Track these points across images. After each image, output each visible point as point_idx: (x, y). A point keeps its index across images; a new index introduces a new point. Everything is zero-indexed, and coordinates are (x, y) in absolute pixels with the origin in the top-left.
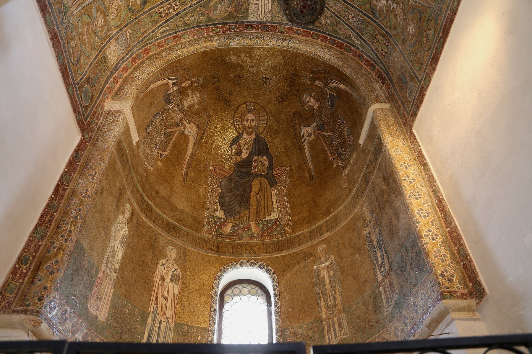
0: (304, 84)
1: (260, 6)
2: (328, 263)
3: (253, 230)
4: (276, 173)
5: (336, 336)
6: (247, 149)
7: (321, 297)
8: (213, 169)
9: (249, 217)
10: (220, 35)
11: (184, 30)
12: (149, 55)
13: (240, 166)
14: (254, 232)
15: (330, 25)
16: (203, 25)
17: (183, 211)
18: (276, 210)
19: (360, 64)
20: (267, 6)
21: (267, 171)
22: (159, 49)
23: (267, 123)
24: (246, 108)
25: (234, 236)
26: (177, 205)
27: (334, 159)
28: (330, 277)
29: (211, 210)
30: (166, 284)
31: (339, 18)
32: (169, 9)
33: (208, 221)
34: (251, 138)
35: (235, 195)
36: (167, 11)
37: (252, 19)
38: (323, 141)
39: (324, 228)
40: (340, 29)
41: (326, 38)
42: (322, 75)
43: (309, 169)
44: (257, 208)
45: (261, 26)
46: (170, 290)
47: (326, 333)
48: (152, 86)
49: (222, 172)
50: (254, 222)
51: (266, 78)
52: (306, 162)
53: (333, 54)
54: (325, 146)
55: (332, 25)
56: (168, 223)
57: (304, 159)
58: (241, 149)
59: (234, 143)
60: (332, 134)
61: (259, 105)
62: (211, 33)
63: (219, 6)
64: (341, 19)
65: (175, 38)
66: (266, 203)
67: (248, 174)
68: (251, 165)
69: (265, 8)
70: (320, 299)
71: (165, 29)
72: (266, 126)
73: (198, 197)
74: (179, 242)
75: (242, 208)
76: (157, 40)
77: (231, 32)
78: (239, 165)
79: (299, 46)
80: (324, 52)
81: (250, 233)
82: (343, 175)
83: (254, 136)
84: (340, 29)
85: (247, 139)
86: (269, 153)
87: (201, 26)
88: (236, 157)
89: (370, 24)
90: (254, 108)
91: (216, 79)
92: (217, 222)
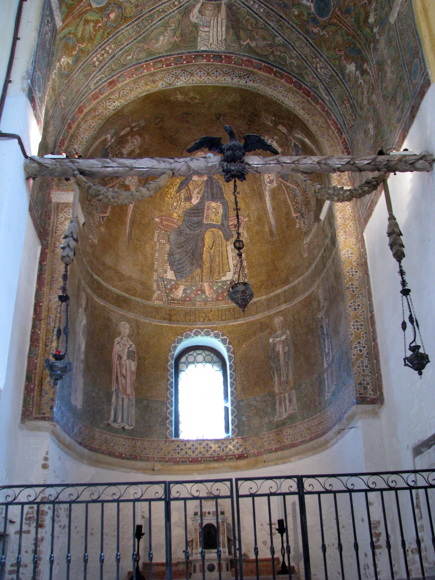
0: (265, 125)
1: (211, 34)
2: (284, 337)
3: (207, 293)
4: (232, 223)
5: (286, 411)
6: (198, 193)
7: (275, 372)
8: (159, 221)
9: (202, 278)
10: (164, 71)
11: (120, 72)
12: (84, 113)
14: (208, 296)
15: (296, 67)
16: (142, 62)
17: (130, 278)
18: (232, 269)
19: (327, 122)
20: (220, 34)
21: (222, 220)
22: (94, 102)
25: (187, 301)
26: (124, 272)
27: (297, 217)
28: (285, 353)
29: (160, 271)
30: (123, 362)
31: (306, 63)
32: (103, 54)
33: (158, 285)
35: (186, 251)
36: (101, 58)
37: (202, 49)
38: (286, 192)
39: (282, 298)
40: (308, 75)
41: (292, 79)
42: (286, 122)
43: (269, 223)
44: (211, 266)
45: (214, 56)
46: (128, 368)
47: (277, 407)
48: (91, 150)
49: (170, 224)
50: (208, 283)
51: (219, 114)
52: (266, 214)
53: (298, 102)
54: (288, 199)
55: (299, 67)
56: (118, 296)
57: (264, 208)
58: (191, 194)
59: (183, 187)
60: (296, 188)
62: (152, 69)
63: (162, 38)
64: (308, 65)
65: (110, 83)
66: (221, 260)
67: (200, 224)
68: (203, 212)
69: (217, 36)
70: (274, 374)
71: (99, 78)
73: (145, 258)
74: (131, 315)
75: (194, 267)
76: (91, 92)
77: (177, 64)
78: (189, 213)
79: (259, 86)
80: (289, 98)
81: (204, 297)
82: (305, 242)
83: (205, 178)
84: (308, 75)
86: (224, 198)
87: (140, 63)
89: (339, 84)
91: (159, 120)
92: (167, 285)
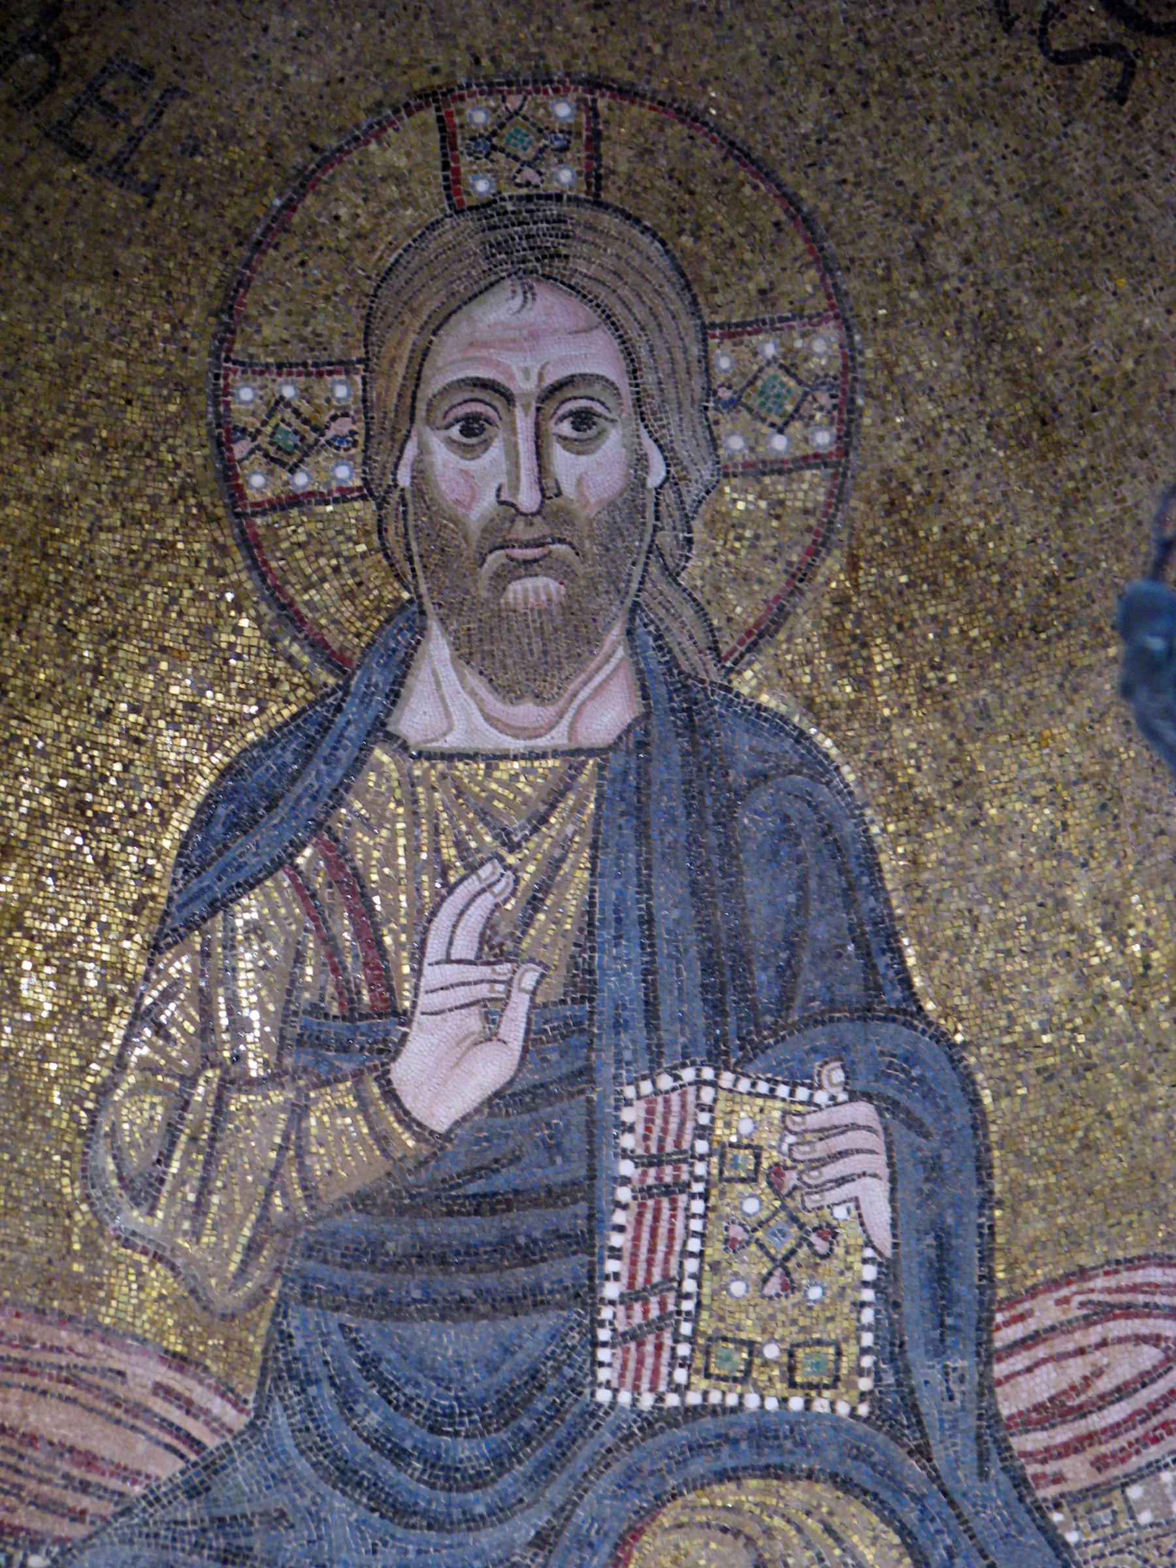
13: (366, 1280)
23: (846, 440)
24: (452, 185)
34: (558, 737)
61: (692, 118)
72: (838, 497)
85: (494, 758)
88: (299, 1111)
90: (595, 178)
